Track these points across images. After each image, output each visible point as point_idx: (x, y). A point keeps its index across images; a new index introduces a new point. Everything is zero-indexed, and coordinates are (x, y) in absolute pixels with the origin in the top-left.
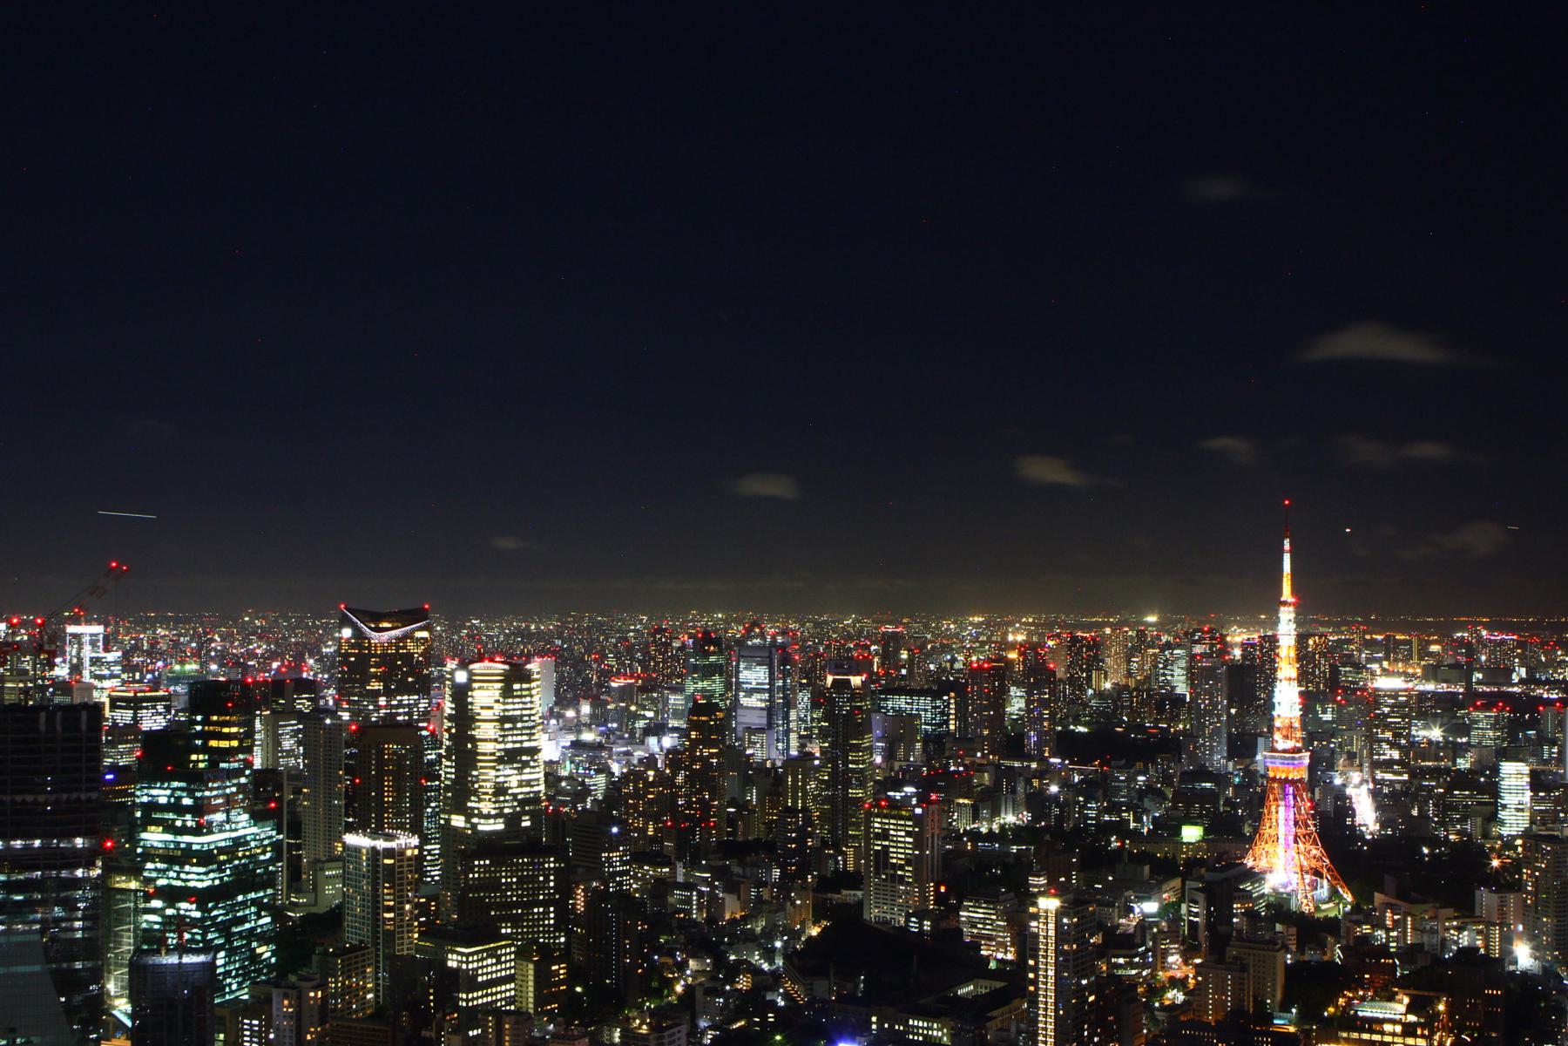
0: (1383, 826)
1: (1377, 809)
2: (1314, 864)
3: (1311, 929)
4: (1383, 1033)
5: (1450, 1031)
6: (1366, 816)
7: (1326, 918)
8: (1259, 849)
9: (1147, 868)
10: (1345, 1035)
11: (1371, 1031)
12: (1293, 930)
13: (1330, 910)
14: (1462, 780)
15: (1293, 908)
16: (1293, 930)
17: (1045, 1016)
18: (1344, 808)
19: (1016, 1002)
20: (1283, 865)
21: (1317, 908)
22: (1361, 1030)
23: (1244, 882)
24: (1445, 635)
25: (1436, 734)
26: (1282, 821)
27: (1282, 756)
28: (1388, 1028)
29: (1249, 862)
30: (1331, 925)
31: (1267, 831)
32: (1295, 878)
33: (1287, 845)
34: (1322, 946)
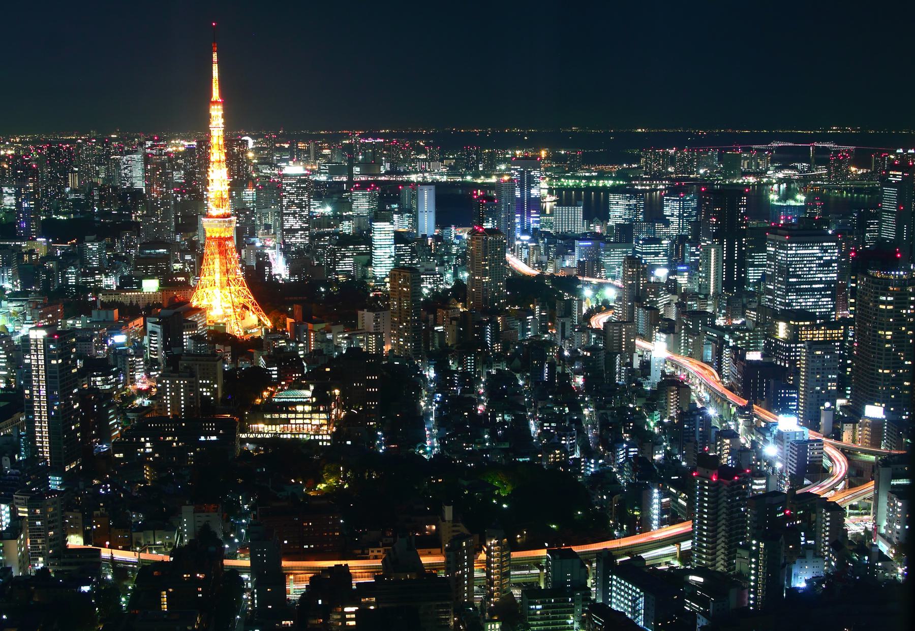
0: (292, 274)
1: (287, 262)
2: (242, 300)
3: (244, 347)
4: (296, 412)
5: (343, 408)
6: (280, 268)
7: (253, 338)
8: (200, 292)
9: (116, 311)
10: (268, 416)
11: (288, 412)
12: (229, 348)
13: (257, 333)
14: (345, 240)
15: (228, 331)
16: (229, 348)
17: (40, 422)
18: (263, 262)
19: (17, 415)
20: (221, 301)
21: (246, 333)
22: (281, 412)
23: (190, 315)
24: (332, 140)
25: (328, 210)
26: (217, 270)
27: (216, 223)
28: (299, 408)
29: (194, 303)
30: (256, 343)
31: (204, 279)
32: (230, 312)
33: (222, 287)
34: (250, 357)
